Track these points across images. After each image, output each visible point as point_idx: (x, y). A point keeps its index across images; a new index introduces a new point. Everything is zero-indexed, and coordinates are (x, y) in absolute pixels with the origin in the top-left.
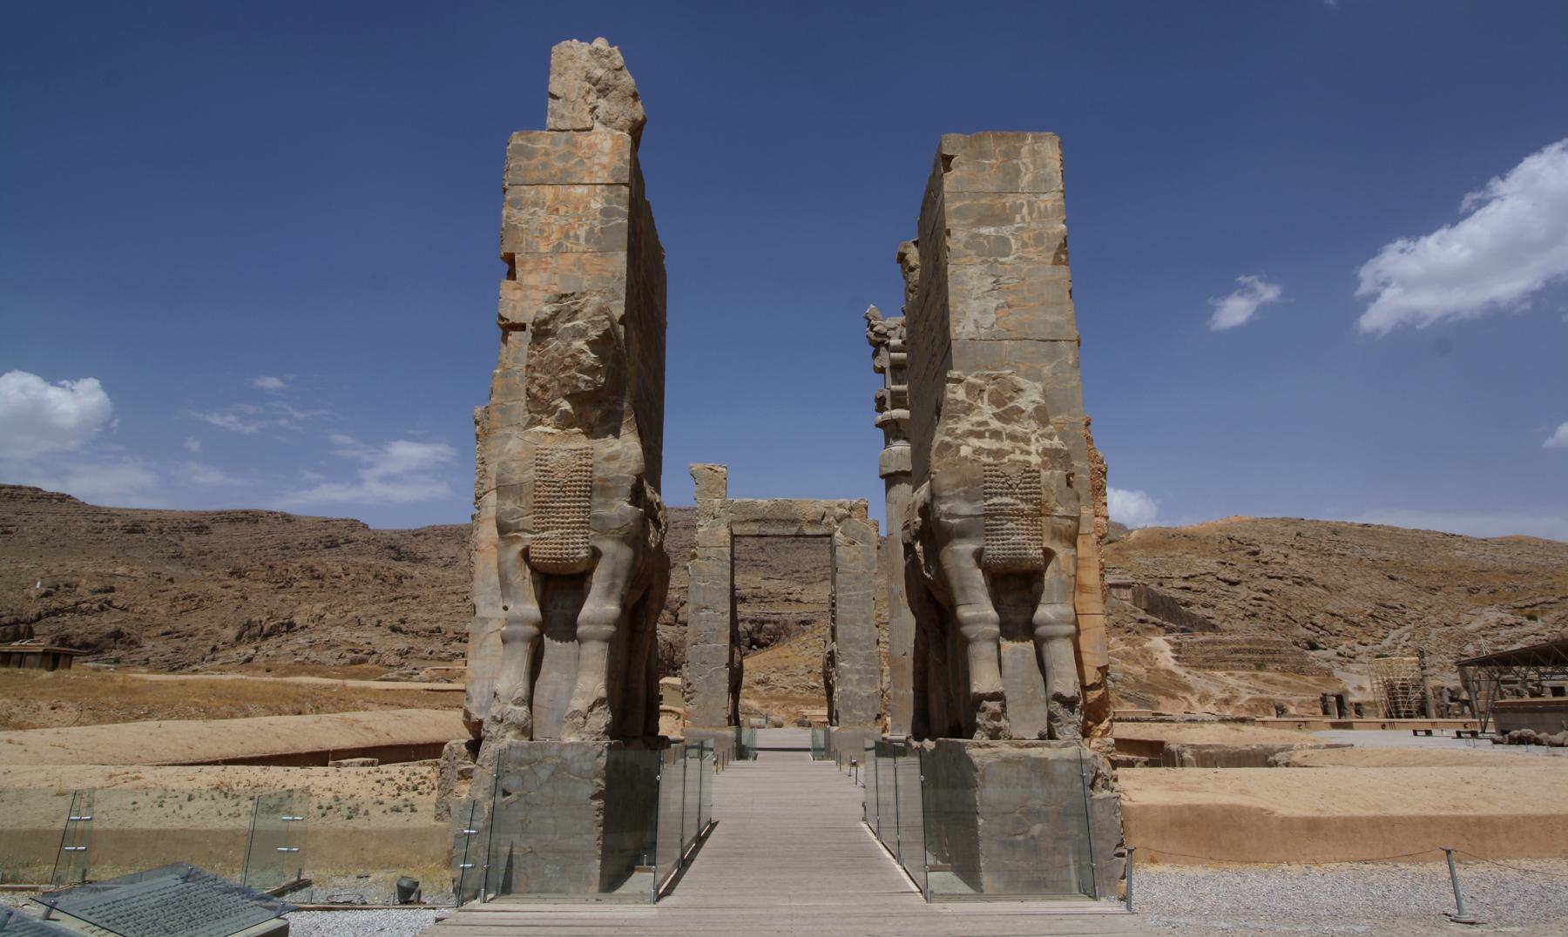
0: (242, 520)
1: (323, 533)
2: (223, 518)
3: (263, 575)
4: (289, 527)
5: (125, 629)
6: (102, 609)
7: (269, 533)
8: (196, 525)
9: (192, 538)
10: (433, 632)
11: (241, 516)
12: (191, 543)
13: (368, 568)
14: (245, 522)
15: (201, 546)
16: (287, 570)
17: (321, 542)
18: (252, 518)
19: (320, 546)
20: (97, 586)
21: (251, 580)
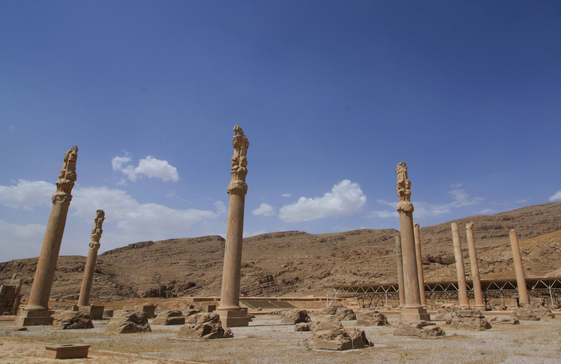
0: (355, 234)
1: (382, 235)
2: (349, 234)
3: (341, 255)
4: (370, 234)
5: (299, 277)
6: (294, 270)
7: (364, 237)
8: (341, 237)
9: (340, 242)
10: (366, 274)
11: (354, 232)
12: (340, 244)
13: (375, 249)
14: (356, 234)
15: (342, 244)
16: (348, 253)
17: (381, 239)
18: (358, 232)
19: (381, 240)
20: (298, 263)
21: (337, 257)
